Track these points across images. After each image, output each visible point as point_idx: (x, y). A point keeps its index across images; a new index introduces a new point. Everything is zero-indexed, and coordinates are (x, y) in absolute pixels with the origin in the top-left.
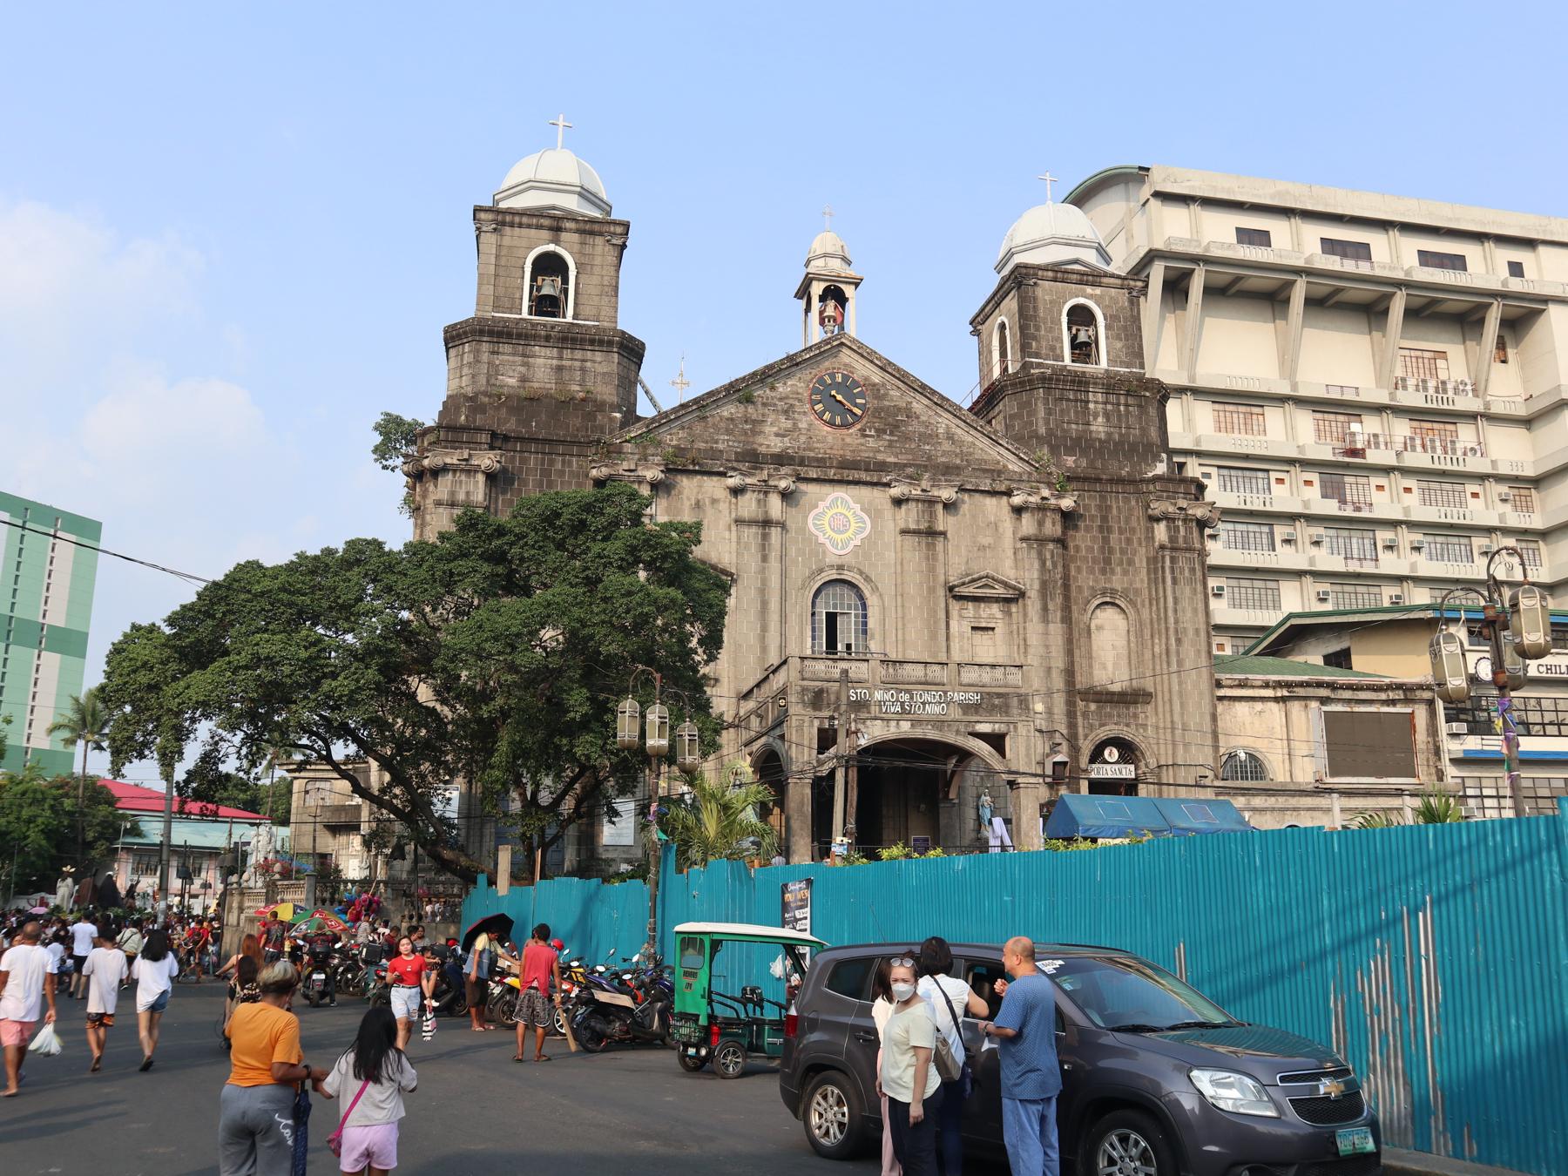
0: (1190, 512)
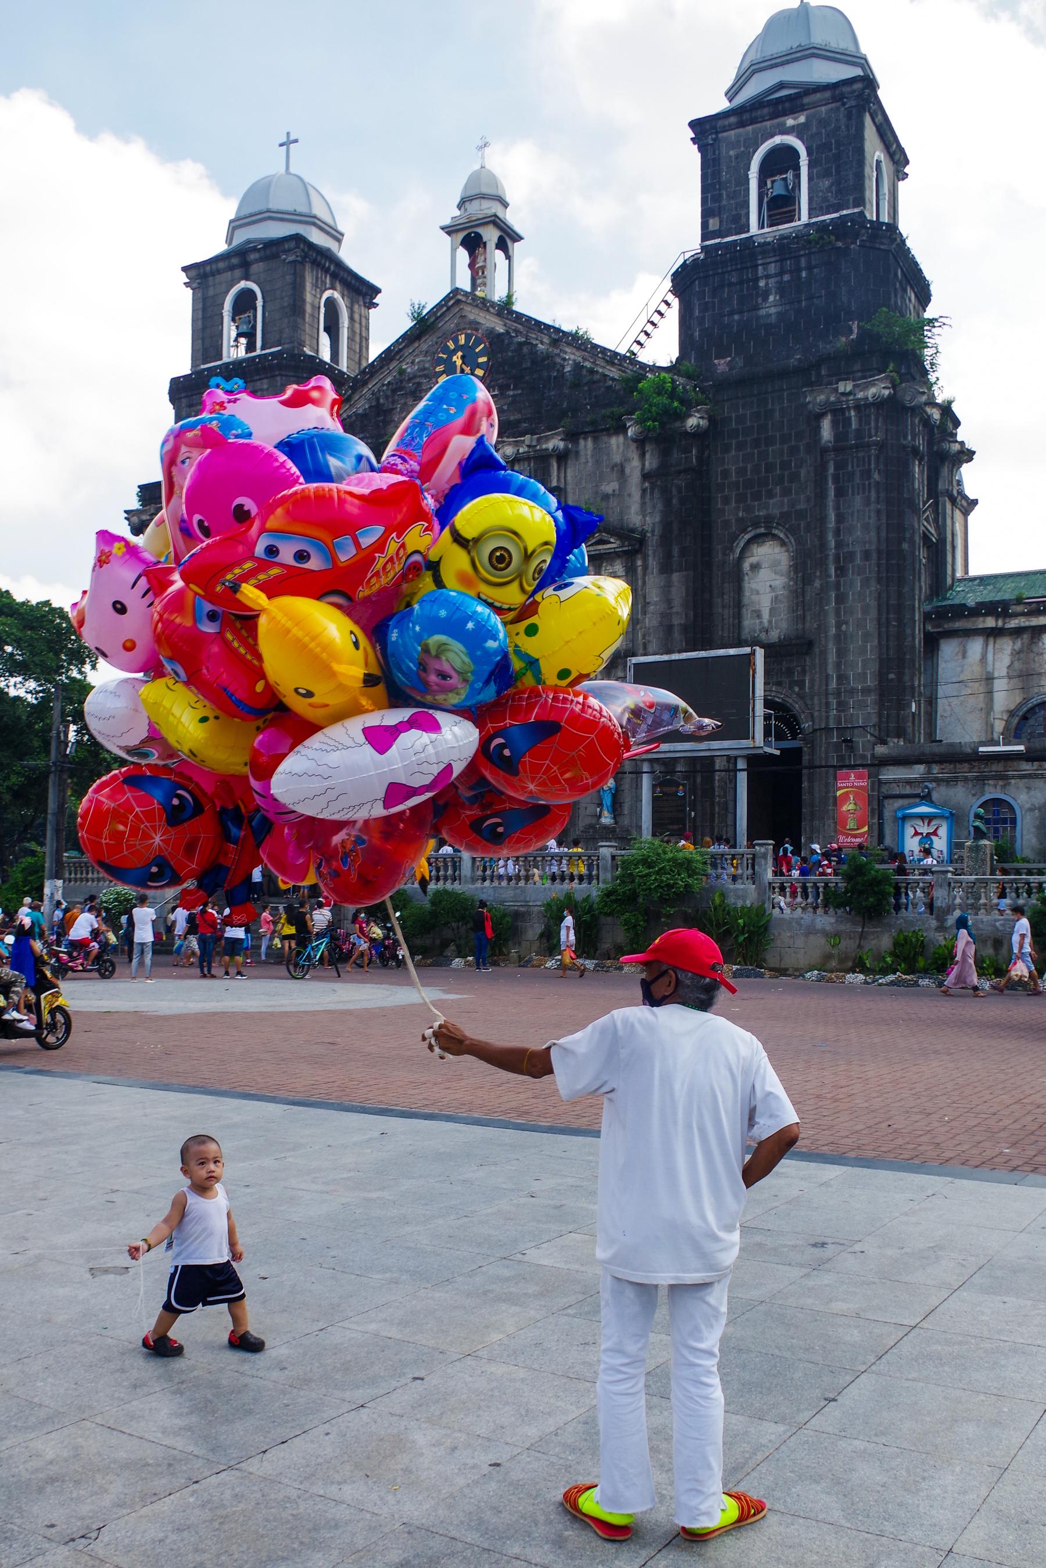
0: (860, 395)
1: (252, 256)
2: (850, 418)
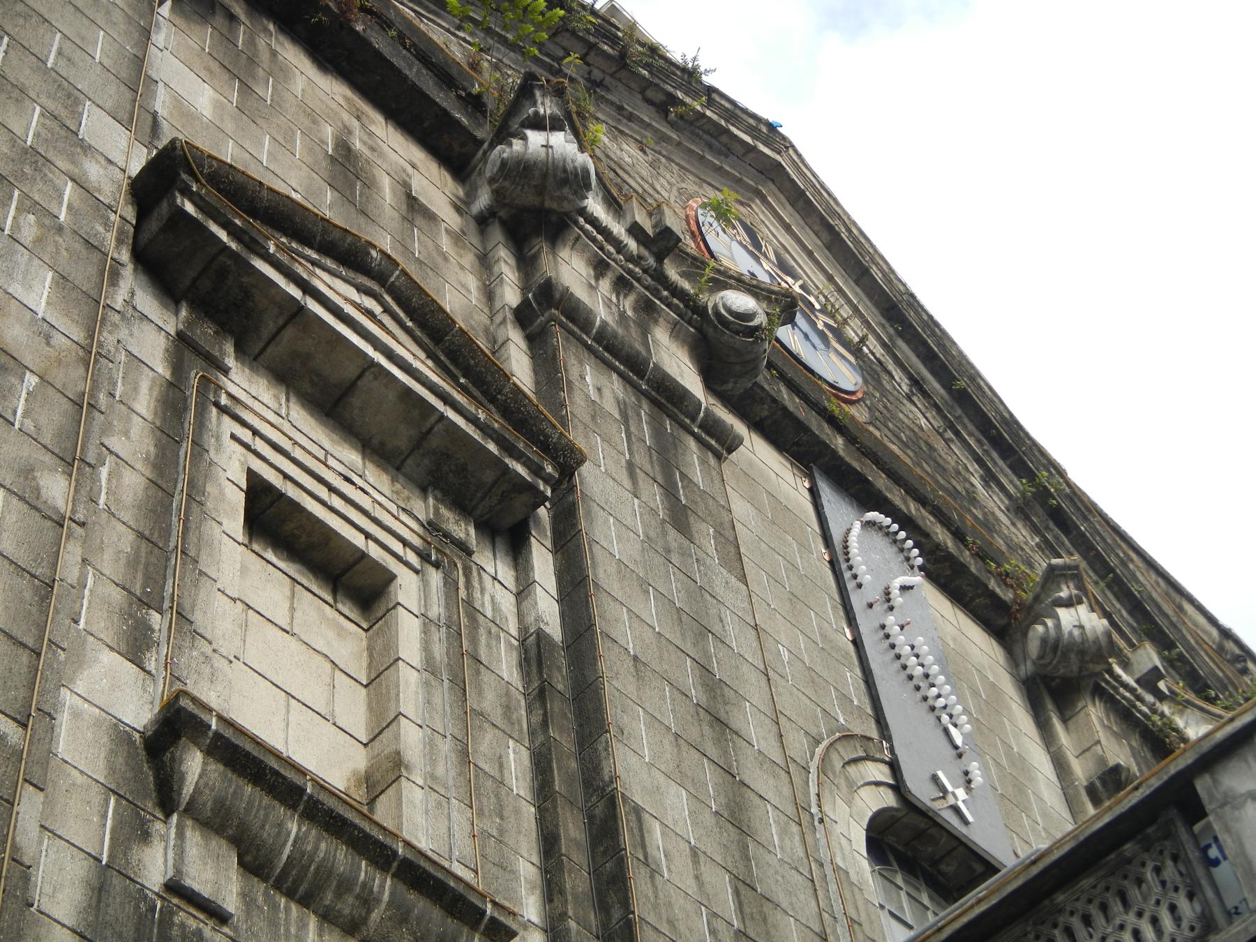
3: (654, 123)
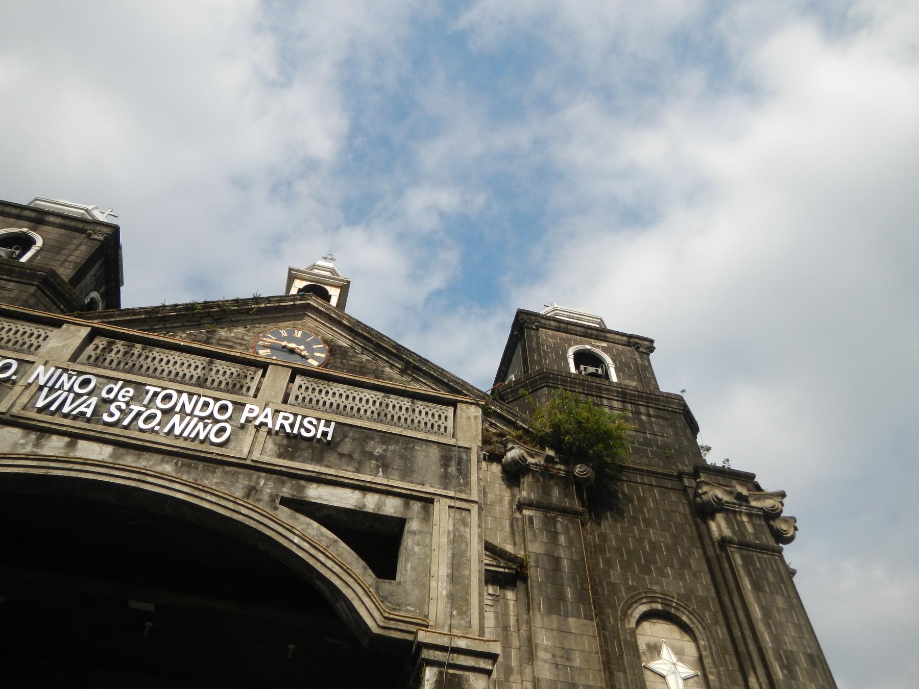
1: (51, 219)
2: (743, 522)
3: (247, 318)
